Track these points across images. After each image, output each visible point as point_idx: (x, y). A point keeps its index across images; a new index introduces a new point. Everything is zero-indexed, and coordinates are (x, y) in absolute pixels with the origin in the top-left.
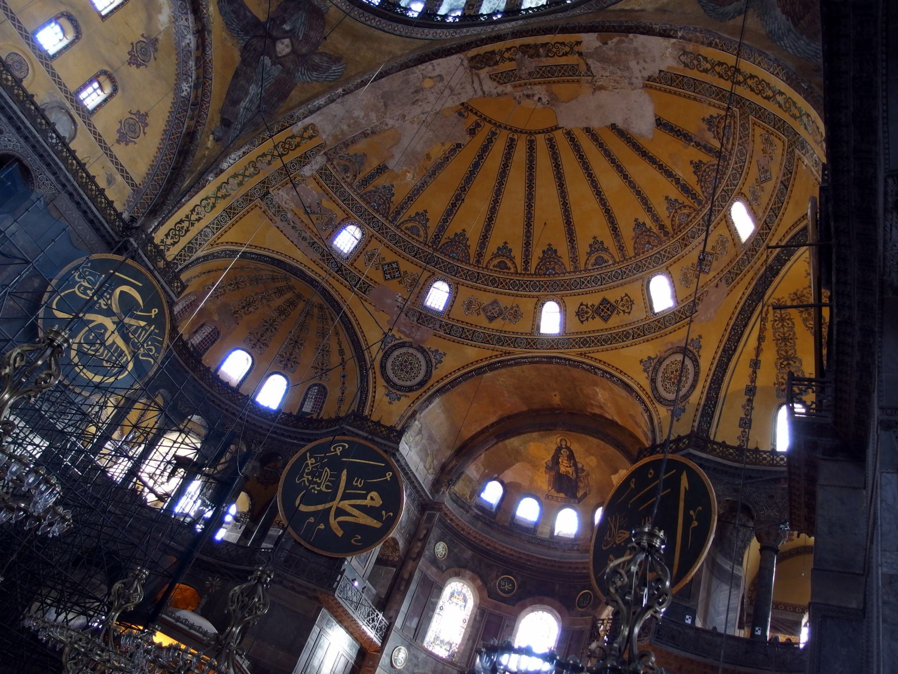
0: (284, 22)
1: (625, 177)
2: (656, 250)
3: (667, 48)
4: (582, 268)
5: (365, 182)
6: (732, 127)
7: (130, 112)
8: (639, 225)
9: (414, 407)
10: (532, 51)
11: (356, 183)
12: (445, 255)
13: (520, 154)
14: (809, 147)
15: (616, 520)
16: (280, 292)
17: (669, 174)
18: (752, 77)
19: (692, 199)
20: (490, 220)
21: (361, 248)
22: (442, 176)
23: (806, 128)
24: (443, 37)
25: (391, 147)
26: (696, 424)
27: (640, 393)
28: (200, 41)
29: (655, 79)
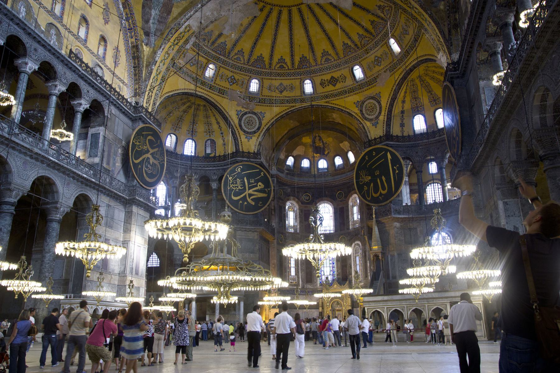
2: (354, 54)
4: (320, 63)
5: (213, 43)
7: (114, 50)
8: (344, 44)
9: (260, 139)
11: (209, 44)
12: (254, 67)
15: (363, 173)
16: (184, 104)
17: (359, 24)
20: (273, 47)
21: (216, 74)
22: (249, 32)
25: (224, 24)
26: (385, 129)
27: (356, 116)
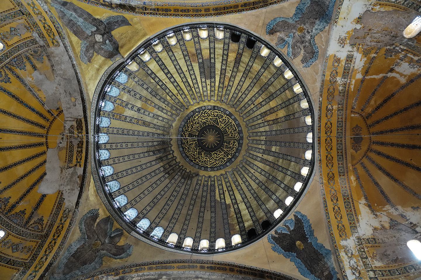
0: (110, 41)
1: (22, 178)
3: (72, 204)
6: (38, 230)
10: (80, 145)
11: (28, 54)
13: (37, 130)
14: (22, 277)
17: (21, 199)
18: (55, 243)
19: (9, 210)
22: (29, 95)
23: (31, 274)
24: (92, 107)
28: (107, 4)
29: (62, 196)
